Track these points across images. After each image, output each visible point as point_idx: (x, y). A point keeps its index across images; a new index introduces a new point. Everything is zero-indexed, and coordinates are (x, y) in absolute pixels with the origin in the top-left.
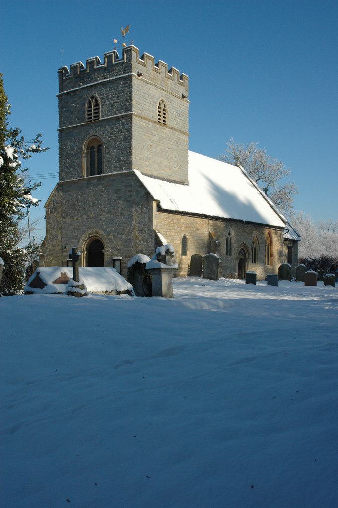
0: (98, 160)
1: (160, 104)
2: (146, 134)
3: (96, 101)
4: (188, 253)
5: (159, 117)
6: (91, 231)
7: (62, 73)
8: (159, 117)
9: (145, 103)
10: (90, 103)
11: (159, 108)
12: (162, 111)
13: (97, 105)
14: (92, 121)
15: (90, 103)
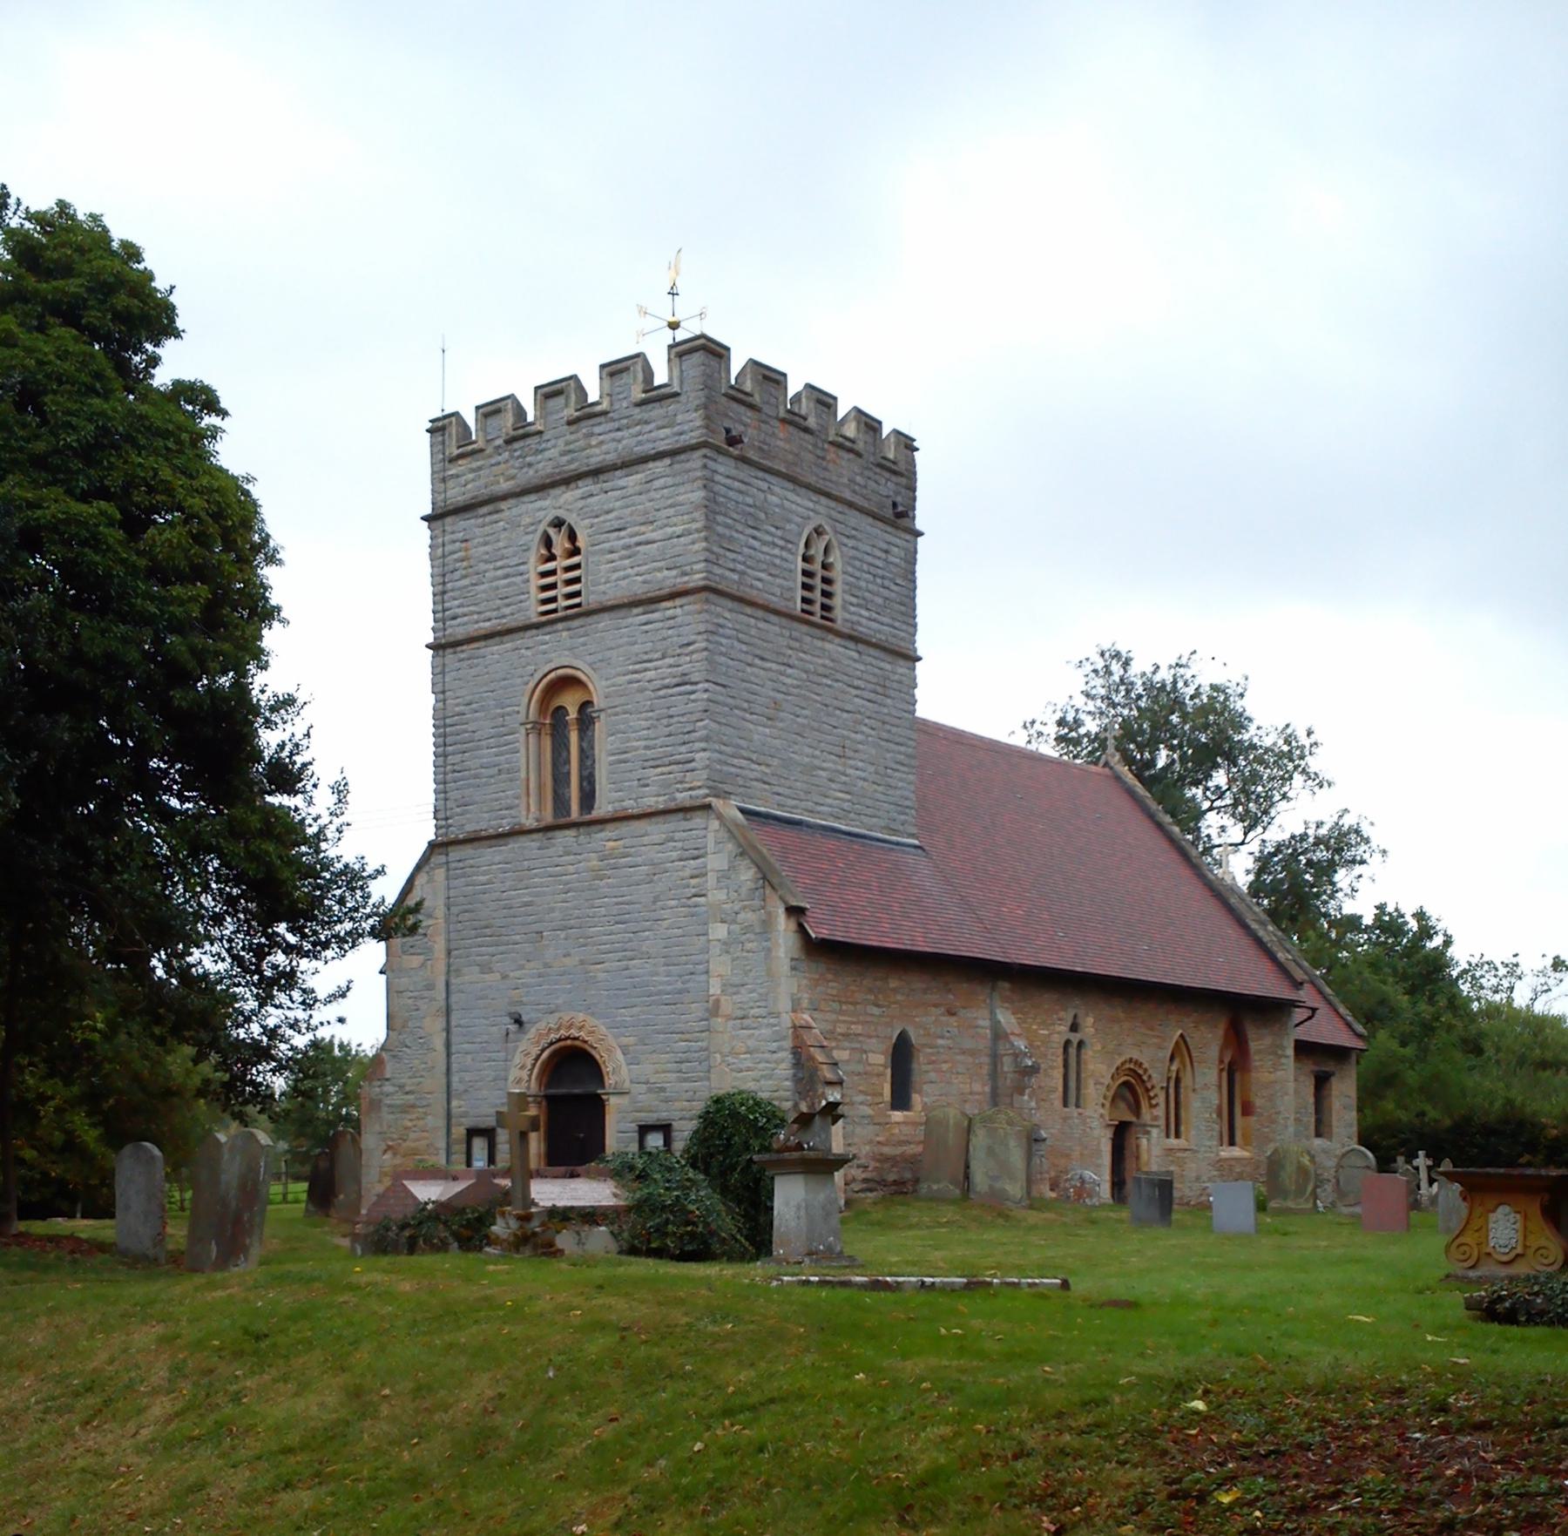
0: (582, 750)
1: (807, 545)
2: (757, 661)
3: (572, 536)
4: (916, 1099)
5: (807, 594)
6: (552, 1021)
7: (440, 428)
8: (807, 594)
9: (751, 541)
10: (548, 542)
11: (806, 559)
12: (816, 567)
13: (575, 551)
14: (555, 611)
15: (548, 542)
